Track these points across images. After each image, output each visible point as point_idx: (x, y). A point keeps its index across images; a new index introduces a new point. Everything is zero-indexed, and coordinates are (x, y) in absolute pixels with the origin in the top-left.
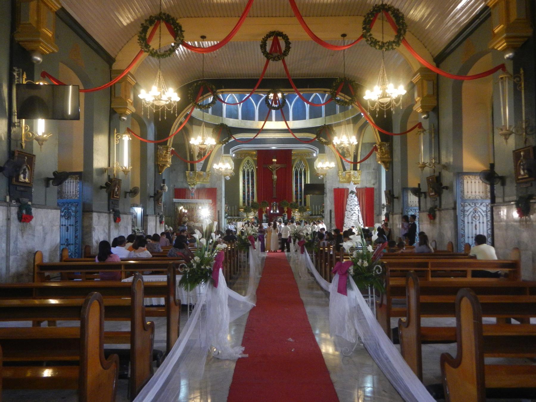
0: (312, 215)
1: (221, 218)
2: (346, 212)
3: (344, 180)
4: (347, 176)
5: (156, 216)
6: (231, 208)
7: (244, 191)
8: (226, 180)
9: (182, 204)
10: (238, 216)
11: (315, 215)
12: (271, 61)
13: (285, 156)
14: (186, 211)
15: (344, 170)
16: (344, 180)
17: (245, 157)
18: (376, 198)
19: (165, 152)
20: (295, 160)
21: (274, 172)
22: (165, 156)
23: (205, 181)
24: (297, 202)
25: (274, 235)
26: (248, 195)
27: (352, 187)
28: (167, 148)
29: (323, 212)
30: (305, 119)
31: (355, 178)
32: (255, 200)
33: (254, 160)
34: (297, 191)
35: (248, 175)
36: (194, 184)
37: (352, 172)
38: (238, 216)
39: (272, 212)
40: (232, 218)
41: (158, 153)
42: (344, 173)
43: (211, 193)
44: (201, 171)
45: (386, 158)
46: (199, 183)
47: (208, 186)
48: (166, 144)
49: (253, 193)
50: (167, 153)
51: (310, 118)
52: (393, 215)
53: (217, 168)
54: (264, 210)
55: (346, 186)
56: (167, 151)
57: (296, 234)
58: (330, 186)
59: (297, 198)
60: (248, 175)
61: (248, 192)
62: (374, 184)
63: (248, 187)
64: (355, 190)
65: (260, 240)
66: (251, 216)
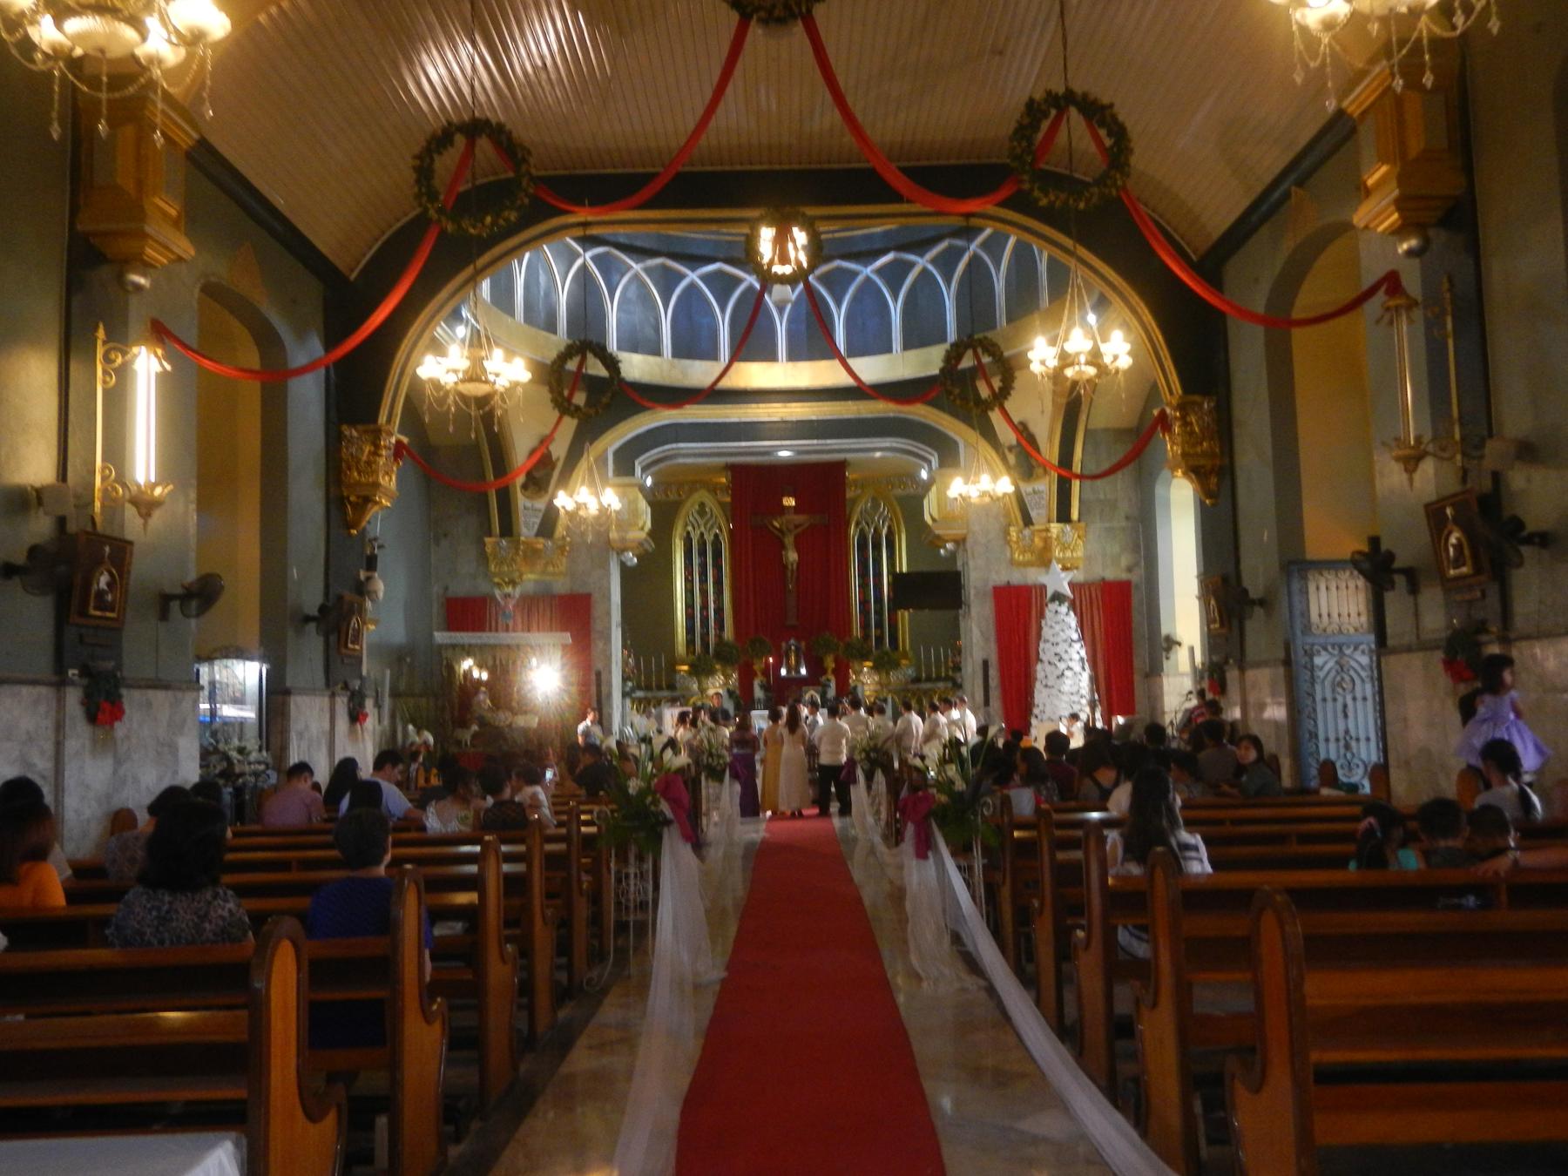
0: (917, 680)
1: (610, 695)
2: (1039, 667)
3: (1028, 556)
4: (1038, 542)
5: (333, 695)
6: (648, 663)
7: (689, 606)
8: (624, 569)
9: (468, 651)
10: (671, 687)
11: (929, 679)
12: (756, 32)
13: (822, 484)
14: (485, 676)
15: (1028, 521)
16: (1028, 556)
17: (692, 490)
18: (1137, 618)
19: (368, 449)
20: (854, 501)
21: (789, 540)
22: (369, 463)
23: (550, 569)
24: (866, 636)
25: (791, 751)
26: (705, 620)
27: (1059, 580)
28: (376, 434)
29: (957, 668)
30: (889, 350)
31: (1064, 548)
32: (729, 633)
33: (722, 504)
34: (864, 603)
35: (703, 553)
36: (513, 583)
37: (1055, 528)
38: (671, 687)
39: (783, 672)
40: (649, 695)
41: (344, 453)
42: (1027, 532)
43: (573, 613)
44: (538, 534)
45: (1204, 454)
46: (530, 579)
47: (561, 586)
48: (375, 420)
49: (719, 611)
50: (376, 453)
51: (908, 345)
52: (1242, 669)
53: (570, 506)
54: (758, 666)
55: (1034, 576)
56: (377, 446)
57: (875, 749)
58: (983, 574)
59: (865, 626)
60: (703, 553)
61: (705, 606)
62: (1129, 570)
63: (704, 593)
64: (1068, 591)
65: (735, 776)
66: (717, 686)
